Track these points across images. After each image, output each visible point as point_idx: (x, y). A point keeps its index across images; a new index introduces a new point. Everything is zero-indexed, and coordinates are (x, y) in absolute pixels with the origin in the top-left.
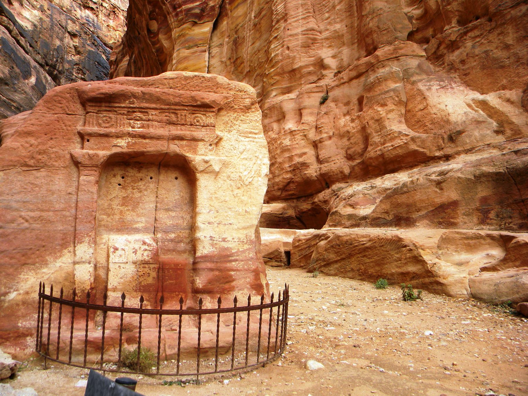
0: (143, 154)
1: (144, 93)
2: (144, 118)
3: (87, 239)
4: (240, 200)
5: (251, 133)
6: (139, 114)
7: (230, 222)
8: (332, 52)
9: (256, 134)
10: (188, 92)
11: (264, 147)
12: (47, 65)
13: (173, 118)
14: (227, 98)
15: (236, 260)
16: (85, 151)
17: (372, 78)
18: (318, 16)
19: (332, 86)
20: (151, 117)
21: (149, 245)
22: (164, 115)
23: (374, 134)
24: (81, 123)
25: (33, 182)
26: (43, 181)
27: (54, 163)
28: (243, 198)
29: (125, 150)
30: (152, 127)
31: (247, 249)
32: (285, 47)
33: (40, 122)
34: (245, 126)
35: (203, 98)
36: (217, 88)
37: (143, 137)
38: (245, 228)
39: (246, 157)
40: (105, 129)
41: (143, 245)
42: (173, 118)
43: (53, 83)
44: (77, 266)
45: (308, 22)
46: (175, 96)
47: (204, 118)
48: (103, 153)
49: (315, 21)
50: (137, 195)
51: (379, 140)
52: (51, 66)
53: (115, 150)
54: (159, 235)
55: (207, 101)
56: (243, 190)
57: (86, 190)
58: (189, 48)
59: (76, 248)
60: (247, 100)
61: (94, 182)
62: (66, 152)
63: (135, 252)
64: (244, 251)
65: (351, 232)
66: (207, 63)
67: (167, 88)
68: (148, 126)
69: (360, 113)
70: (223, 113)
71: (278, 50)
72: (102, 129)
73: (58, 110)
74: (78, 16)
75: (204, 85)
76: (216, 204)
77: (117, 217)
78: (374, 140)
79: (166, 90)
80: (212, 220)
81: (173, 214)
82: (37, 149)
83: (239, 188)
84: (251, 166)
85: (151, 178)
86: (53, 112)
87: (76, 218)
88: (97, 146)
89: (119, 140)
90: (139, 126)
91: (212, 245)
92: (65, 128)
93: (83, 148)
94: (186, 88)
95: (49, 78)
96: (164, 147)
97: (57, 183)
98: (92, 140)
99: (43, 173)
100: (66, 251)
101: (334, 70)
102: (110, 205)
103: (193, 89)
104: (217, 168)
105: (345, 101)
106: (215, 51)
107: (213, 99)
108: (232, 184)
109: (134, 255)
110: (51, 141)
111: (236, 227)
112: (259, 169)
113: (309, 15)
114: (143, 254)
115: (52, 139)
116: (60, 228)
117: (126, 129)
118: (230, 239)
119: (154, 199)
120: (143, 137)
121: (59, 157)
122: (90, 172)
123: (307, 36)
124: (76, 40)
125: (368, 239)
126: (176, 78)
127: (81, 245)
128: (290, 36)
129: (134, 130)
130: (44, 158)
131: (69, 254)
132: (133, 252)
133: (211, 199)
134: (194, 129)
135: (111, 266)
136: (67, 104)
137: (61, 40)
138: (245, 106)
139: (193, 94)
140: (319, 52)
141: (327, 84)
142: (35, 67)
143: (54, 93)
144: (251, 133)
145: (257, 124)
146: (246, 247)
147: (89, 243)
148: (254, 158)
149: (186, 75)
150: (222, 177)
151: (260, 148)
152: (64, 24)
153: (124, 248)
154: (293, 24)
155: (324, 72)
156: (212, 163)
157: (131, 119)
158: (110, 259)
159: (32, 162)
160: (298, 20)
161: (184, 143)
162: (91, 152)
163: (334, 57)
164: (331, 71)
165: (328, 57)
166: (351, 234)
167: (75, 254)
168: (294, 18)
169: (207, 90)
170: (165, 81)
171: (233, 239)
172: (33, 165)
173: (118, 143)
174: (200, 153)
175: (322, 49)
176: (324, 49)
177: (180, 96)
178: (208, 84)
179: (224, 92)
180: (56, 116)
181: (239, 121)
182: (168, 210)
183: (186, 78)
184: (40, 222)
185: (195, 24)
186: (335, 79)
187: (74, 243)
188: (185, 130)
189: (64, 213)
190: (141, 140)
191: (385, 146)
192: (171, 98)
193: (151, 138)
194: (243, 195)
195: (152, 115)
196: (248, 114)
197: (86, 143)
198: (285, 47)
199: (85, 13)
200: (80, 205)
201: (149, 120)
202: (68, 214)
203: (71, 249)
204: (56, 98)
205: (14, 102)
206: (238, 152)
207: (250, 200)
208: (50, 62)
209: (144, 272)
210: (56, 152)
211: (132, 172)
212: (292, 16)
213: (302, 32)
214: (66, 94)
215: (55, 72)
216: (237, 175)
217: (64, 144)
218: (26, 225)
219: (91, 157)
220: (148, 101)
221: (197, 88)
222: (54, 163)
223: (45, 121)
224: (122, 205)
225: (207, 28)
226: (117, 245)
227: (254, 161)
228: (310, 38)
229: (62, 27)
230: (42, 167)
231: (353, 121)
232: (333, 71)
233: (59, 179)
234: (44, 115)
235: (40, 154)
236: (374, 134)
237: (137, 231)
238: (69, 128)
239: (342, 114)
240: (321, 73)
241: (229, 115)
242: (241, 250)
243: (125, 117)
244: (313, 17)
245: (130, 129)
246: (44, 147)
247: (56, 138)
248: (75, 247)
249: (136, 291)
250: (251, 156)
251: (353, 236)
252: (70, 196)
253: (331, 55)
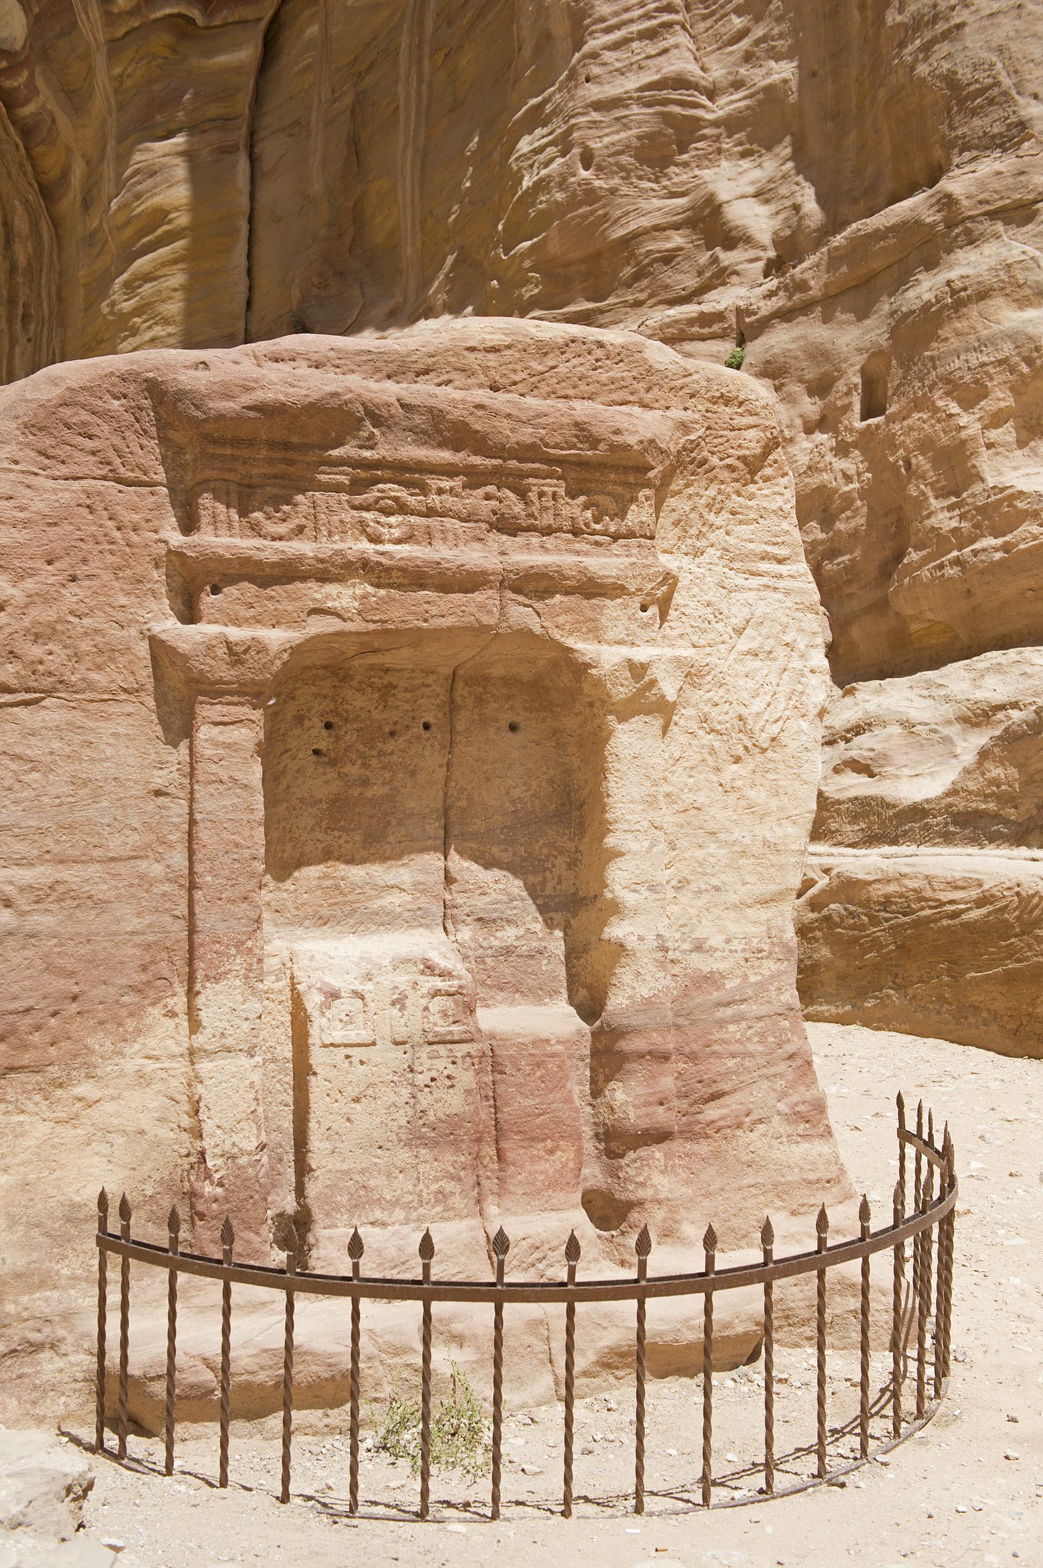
2: (412, 501)
3: (238, 963)
4: (743, 803)
5: (765, 557)
7: (715, 881)
8: (757, 174)
9: (780, 561)
10: (561, 404)
11: (811, 609)
14: (684, 427)
15: (736, 1019)
17: (926, 288)
18: (702, 26)
19: (763, 312)
20: (434, 500)
22: (481, 492)
23: (935, 503)
25: (18, 750)
26: (56, 745)
27: (95, 676)
28: (752, 794)
30: (444, 540)
31: (772, 977)
32: (576, 151)
33: (22, 509)
34: (744, 530)
35: (617, 432)
36: (648, 390)
39: (754, 645)
40: (278, 544)
41: (423, 973)
44: (204, 1066)
45: (665, 51)
46: (519, 420)
49: (693, 48)
51: (954, 524)
53: (319, 626)
54: (465, 934)
56: (751, 767)
57: (225, 778)
59: (200, 1001)
60: (752, 433)
61: (251, 747)
62: (133, 632)
63: (400, 1002)
65: (905, 870)
66: (244, 201)
67: (481, 386)
68: (429, 537)
69: (872, 421)
71: (546, 164)
72: (266, 542)
73: (88, 464)
75: (604, 377)
76: (667, 817)
78: (933, 521)
79: (482, 396)
82: (27, 622)
83: (737, 760)
84: (773, 678)
85: (427, 727)
86: (64, 470)
87: (192, 887)
88: (251, 612)
89: (332, 589)
90: (397, 533)
91: (662, 965)
92: (117, 534)
93: (190, 614)
94: (544, 388)
96: (490, 612)
97: (109, 751)
99: (51, 713)
100: (156, 1011)
101: (764, 248)
103: (571, 392)
104: (670, 692)
105: (811, 374)
106: (270, 149)
107: (649, 436)
108: (716, 744)
109: (395, 1011)
110: (73, 588)
111: (733, 898)
112: (800, 688)
113: (666, 17)
114: (426, 1009)
115: (74, 579)
117: (350, 543)
118: (716, 941)
121: (109, 653)
122: (233, 709)
123: (658, 108)
125: (974, 893)
126: (508, 347)
127: (218, 987)
128: (598, 106)
129: (380, 548)
130: (52, 656)
131: (170, 1023)
132: (393, 1004)
133: (651, 802)
134: (586, 547)
135: (317, 1057)
136: (117, 441)
138: (742, 459)
139: (582, 409)
140: (707, 174)
141: (741, 303)
143: (57, 391)
145: (785, 525)
146: (770, 967)
147: (246, 977)
148: (781, 652)
149: (540, 335)
150: (682, 722)
151: (799, 615)
153: (359, 988)
154: (608, 56)
155: (727, 258)
156: (656, 672)
157: (367, 509)
158: (314, 1031)
160: (626, 41)
162: (235, 633)
163: (762, 195)
164: (752, 253)
165: (743, 197)
166: (904, 876)
167: (195, 1025)
168: (608, 30)
169: (615, 396)
170: (471, 356)
171: (728, 941)
172: (13, 682)
173: (328, 597)
174: (610, 635)
175: (714, 164)
176: (724, 163)
178: (617, 372)
179: (674, 402)
180: (76, 485)
181: (726, 514)
183: (543, 349)
184: (54, 907)
186: (773, 283)
187: (191, 979)
188: (558, 550)
189: (143, 865)
191: (977, 546)
192: (505, 425)
194: (753, 786)
195: (440, 491)
196: (752, 488)
198: (576, 151)
200: (203, 834)
201: (430, 512)
202: (157, 869)
204: (66, 412)
206: (730, 630)
207: (774, 803)
209: (434, 1074)
210: (97, 631)
212: (603, 20)
213: (640, 89)
214: (107, 397)
216: (732, 714)
217: (123, 600)
219: (236, 654)
220: (423, 437)
221: (583, 387)
222: (95, 676)
223: (38, 506)
224: (330, 829)
226: (335, 982)
227: (781, 662)
228: (667, 119)
230: (49, 692)
231: (842, 450)
232: (762, 254)
233: (115, 735)
234: (31, 480)
236: (935, 503)
238: (135, 538)
239: (799, 422)
240: (715, 260)
241: (691, 490)
242: (753, 979)
243: (345, 497)
244: (684, 27)
245: (365, 546)
246: (49, 614)
247: (88, 577)
248: (191, 993)
249: (408, 1144)
250: (771, 642)
251: (911, 884)
252: (161, 800)
253: (751, 190)
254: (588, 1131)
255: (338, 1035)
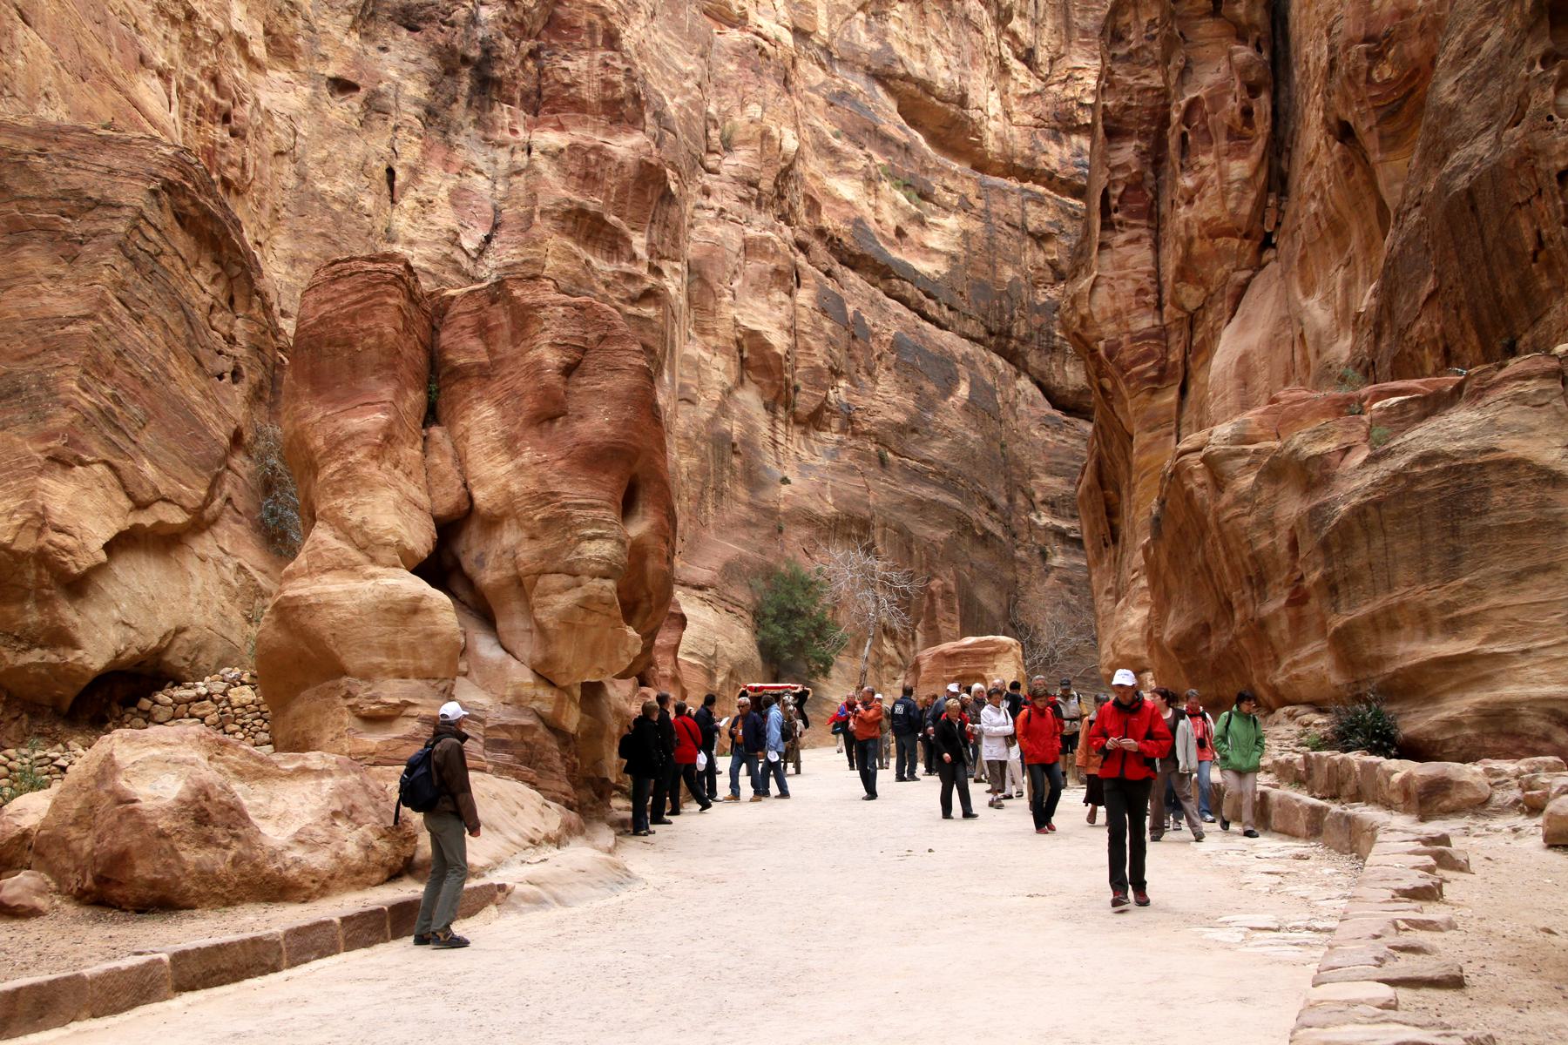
12: (991, 334)
43: (1010, 370)
52: (1000, 334)
58: (1150, 430)
74: (1055, 164)
95: (999, 362)
124: (1050, 246)
137: (1015, 262)
142: (965, 357)
152: (1017, 219)
185: (1154, 391)
199: (1070, 146)
205: (930, 462)
208: (995, 326)
215: (1014, 343)
225: (1171, 397)
229: (1014, 227)
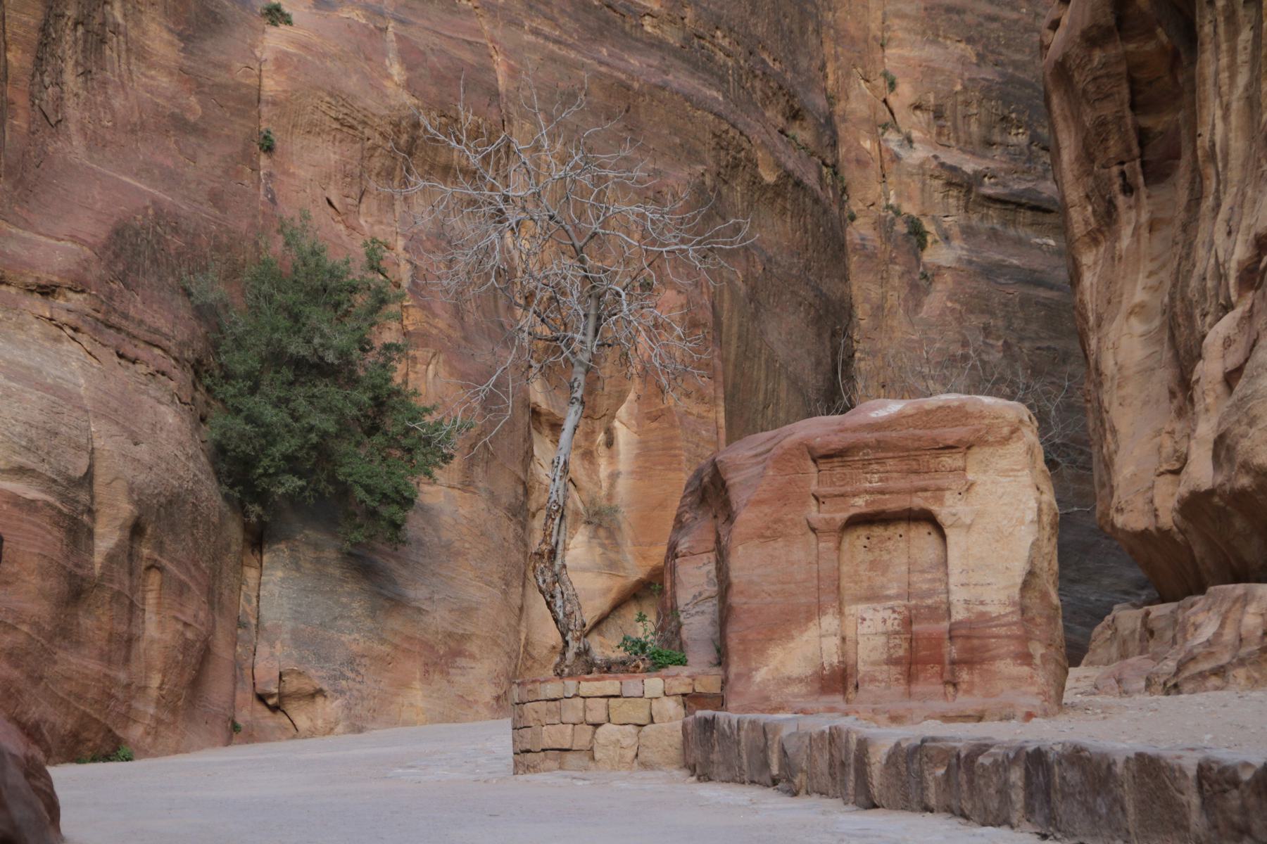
0: (883, 512)
1: (879, 442)
3: (831, 611)
5: (1013, 470)
6: (875, 467)
10: (928, 432)
13: (914, 465)
14: (979, 431)
15: (996, 626)
16: (821, 515)
21: (899, 613)
24: (814, 482)
29: (864, 510)
37: (882, 492)
38: (1005, 588)
42: (914, 465)
47: (950, 461)
48: (841, 516)
50: (886, 557)
53: (853, 511)
55: (950, 442)
64: (1004, 616)
68: (887, 479)
70: (975, 450)
77: (865, 585)
79: (904, 433)
80: (965, 581)
81: (929, 576)
89: (856, 499)
91: (968, 610)
98: (827, 501)
99: (780, 543)
102: (856, 571)
116: (803, 600)
118: (988, 601)
119: (905, 560)
120: (882, 492)
130: (780, 527)
135: (860, 639)
144: (1013, 470)
146: (1009, 609)
149: (927, 407)
159: (768, 533)
161: (929, 494)
162: (827, 516)
177: (920, 439)
182: (922, 572)
190: (880, 496)
192: (909, 443)
193: (891, 493)
197: (822, 506)
203: (816, 621)
211: (878, 531)
218: (769, 599)
219: (827, 522)
220: (884, 450)
235: (775, 522)
237: (889, 598)
245: (868, 485)
254: (947, 662)
255: (866, 630)
